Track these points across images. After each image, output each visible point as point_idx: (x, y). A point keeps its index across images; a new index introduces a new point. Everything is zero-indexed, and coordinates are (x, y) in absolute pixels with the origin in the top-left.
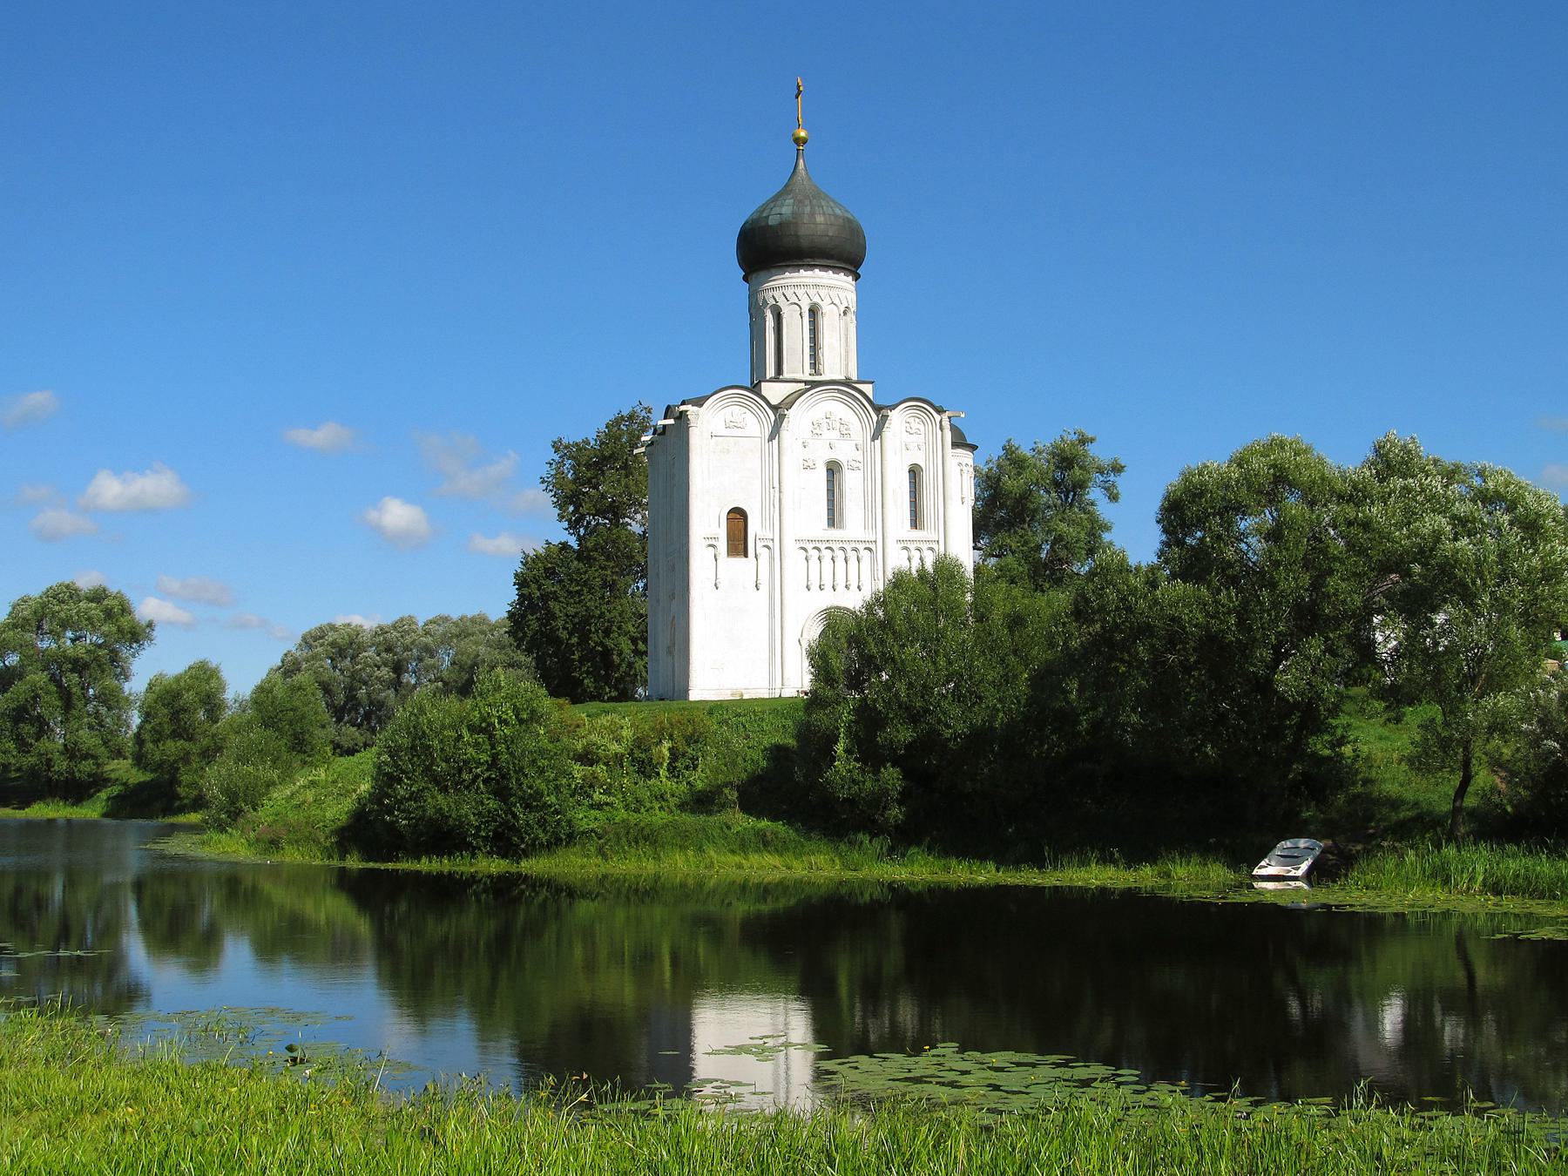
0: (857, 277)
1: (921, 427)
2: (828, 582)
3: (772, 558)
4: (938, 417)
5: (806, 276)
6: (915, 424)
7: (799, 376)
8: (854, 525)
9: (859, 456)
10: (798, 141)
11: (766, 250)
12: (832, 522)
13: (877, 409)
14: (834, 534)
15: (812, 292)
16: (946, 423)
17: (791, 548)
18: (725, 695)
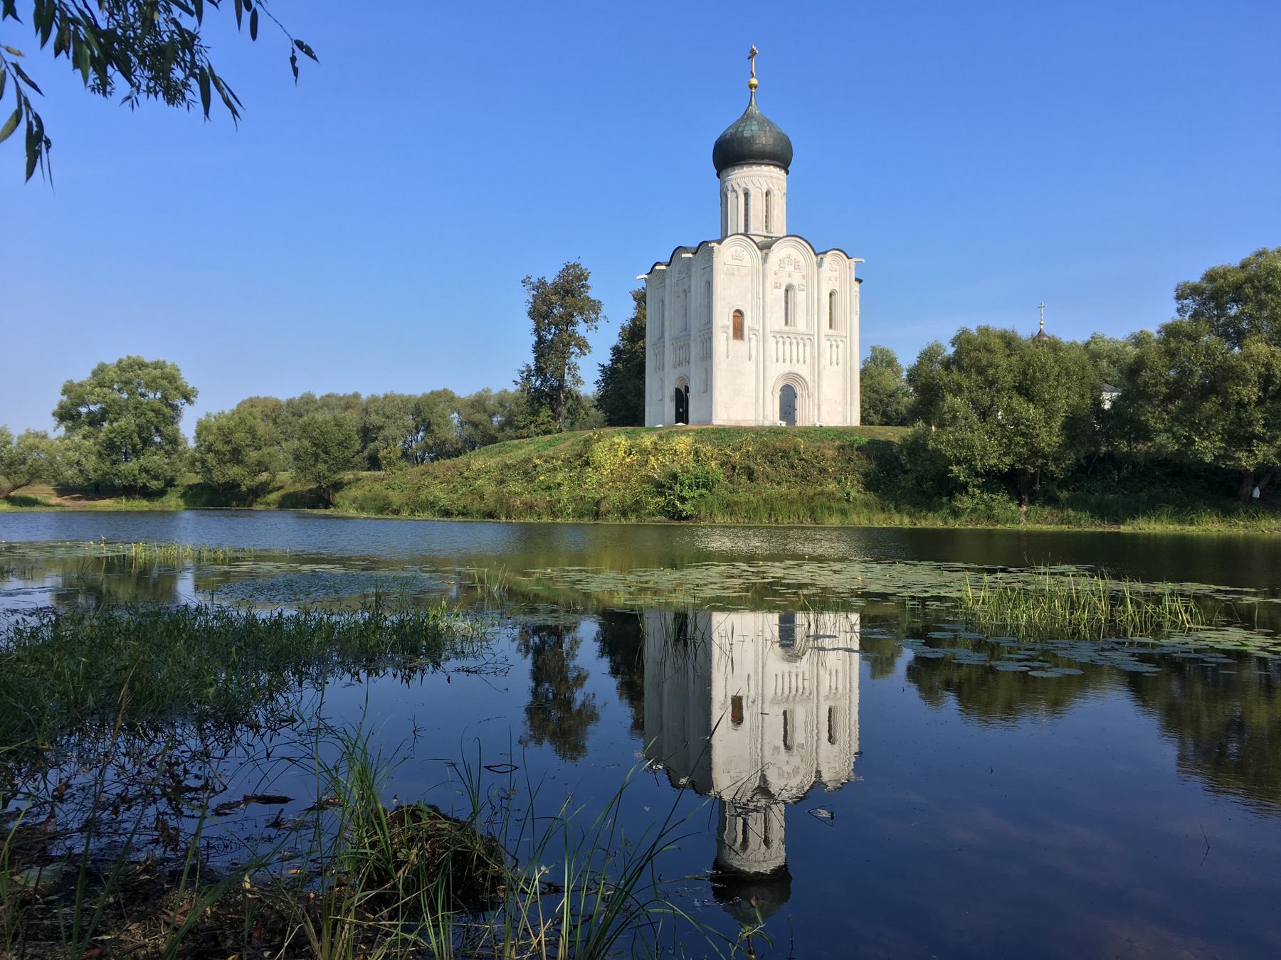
0: (787, 173)
2: (788, 358)
3: (758, 341)
8: (801, 324)
10: (751, 86)
11: (730, 154)
12: (787, 323)
13: (816, 255)
14: (787, 329)
16: (853, 265)
17: (769, 335)
18: (732, 424)
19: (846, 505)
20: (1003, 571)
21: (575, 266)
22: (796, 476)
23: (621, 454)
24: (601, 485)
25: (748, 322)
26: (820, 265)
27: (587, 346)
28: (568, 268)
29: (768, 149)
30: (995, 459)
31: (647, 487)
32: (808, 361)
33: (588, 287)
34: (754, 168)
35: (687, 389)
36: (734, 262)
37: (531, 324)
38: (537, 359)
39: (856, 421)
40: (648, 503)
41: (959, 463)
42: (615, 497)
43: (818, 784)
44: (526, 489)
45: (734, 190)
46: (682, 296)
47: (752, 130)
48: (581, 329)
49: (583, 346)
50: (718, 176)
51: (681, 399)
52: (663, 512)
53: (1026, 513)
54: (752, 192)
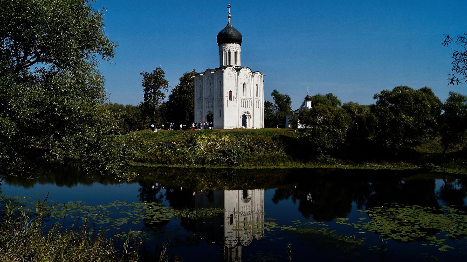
6: (257, 77)
9: (249, 82)
13: (253, 73)
14: (244, 97)
19: (283, 159)
22: (265, 149)
23: (206, 141)
24: (202, 153)
25: (233, 95)
26: (253, 77)
28: (157, 69)
30: (329, 146)
31: (220, 154)
33: (164, 76)
35: (212, 116)
36: (230, 75)
37: (144, 88)
38: (145, 100)
40: (221, 159)
41: (320, 147)
42: (209, 158)
43: (255, 239)
44: (173, 153)
45: (225, 51)
46: (209, 85)
47: (231, 32)
51: (210, 118)
52: (226, 162)
53: (336, 160)
54: (231, 51)
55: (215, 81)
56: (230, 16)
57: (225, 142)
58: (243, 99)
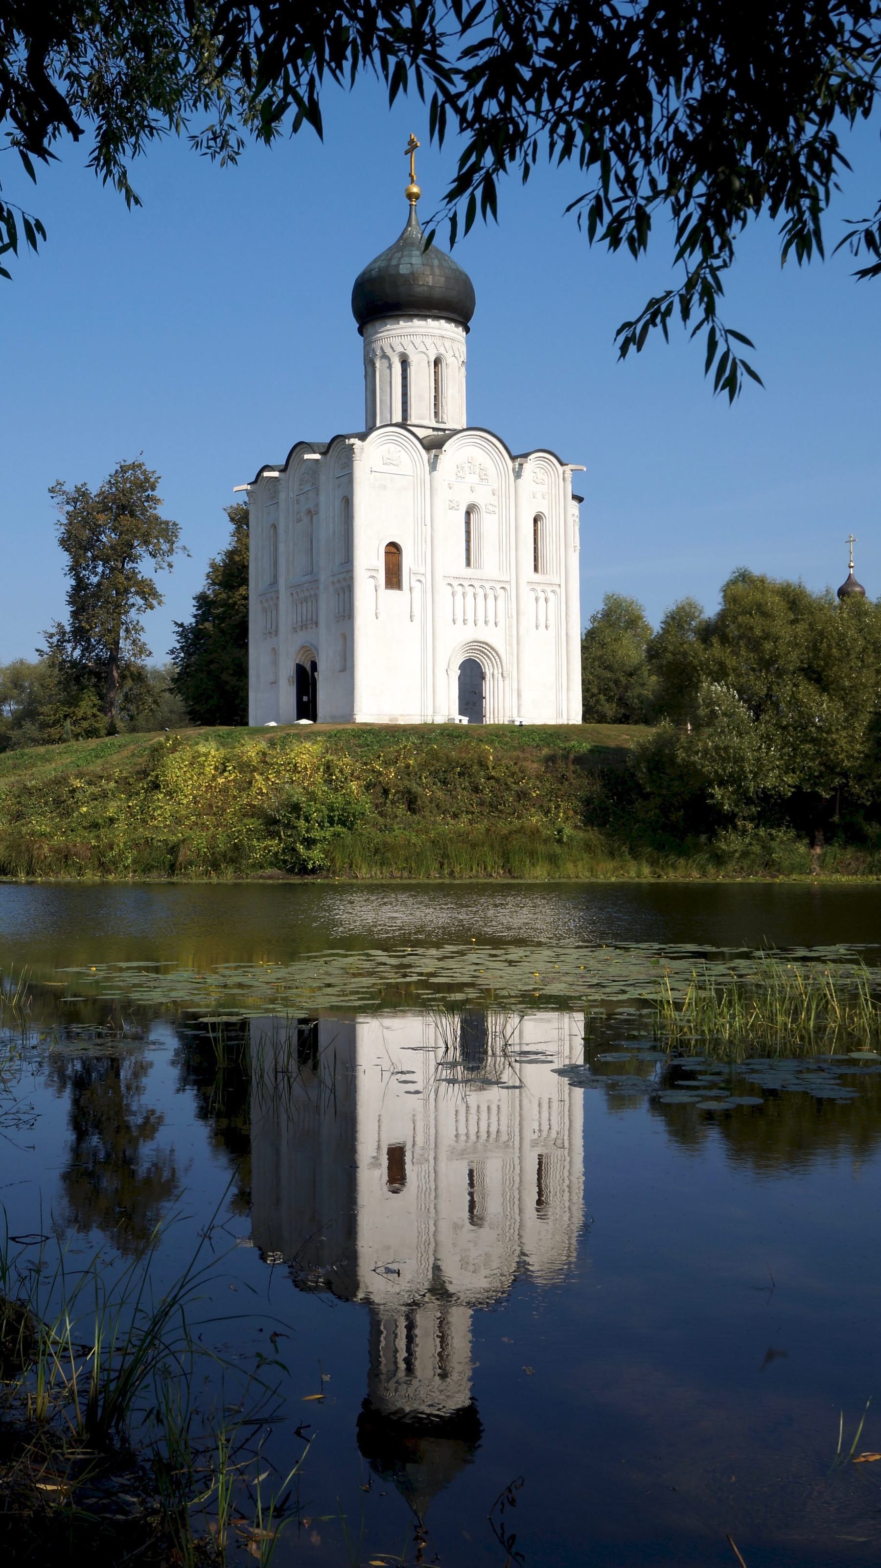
0: (467, 330)
1: (545, 478)
2: (470, 617)
3: (424, 592)
4: (560, 469)
5: (418, 326)
6: (541, 474)
7: (426, 423)
10: (410, 196)
12: (468, 564)
13: (513, 458)
14: (469, 572)
15: (439, 342)
16: (569, 475)
17: (441, 584)
18: (385, 720)
19: (557, 848)
20: (747, 956)
21: (134, 467)
22: (482, 804)
23: (210, 770)
25: (408, 562)
26: (518, 474)
27: (155, 594)
28: (123, 469)
29: (437, 294)
30: (778, 780)
31: (252, 823)
32: (501, 624)
33: (157, 501)
34: (416, 322)
35: (314, 666)
36: (385, 468)
37: (65, 559)
38: (75, 615)
39: (574, 715)
40: (252, 848)
41: (722, 783)
42: (200, 840)
43: (522, 1276)
44: (57, 827)
45: (385, 356)
46: (306, 520)
47: (412, 263)
48: (145, 567)
49: (148, 592)
50: (361, 331)
51: (306, 682)
52: (276, 862)
53: (819, 856)
54: (413, 359)
55: (322, 498)
56: (415, 189)
57: (295, 769)
58: (456, 584)
